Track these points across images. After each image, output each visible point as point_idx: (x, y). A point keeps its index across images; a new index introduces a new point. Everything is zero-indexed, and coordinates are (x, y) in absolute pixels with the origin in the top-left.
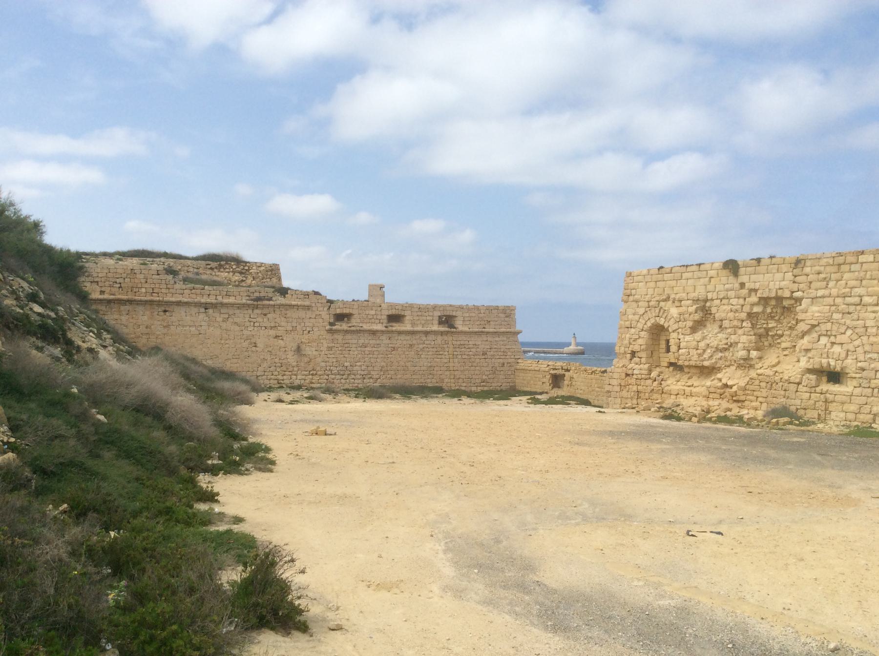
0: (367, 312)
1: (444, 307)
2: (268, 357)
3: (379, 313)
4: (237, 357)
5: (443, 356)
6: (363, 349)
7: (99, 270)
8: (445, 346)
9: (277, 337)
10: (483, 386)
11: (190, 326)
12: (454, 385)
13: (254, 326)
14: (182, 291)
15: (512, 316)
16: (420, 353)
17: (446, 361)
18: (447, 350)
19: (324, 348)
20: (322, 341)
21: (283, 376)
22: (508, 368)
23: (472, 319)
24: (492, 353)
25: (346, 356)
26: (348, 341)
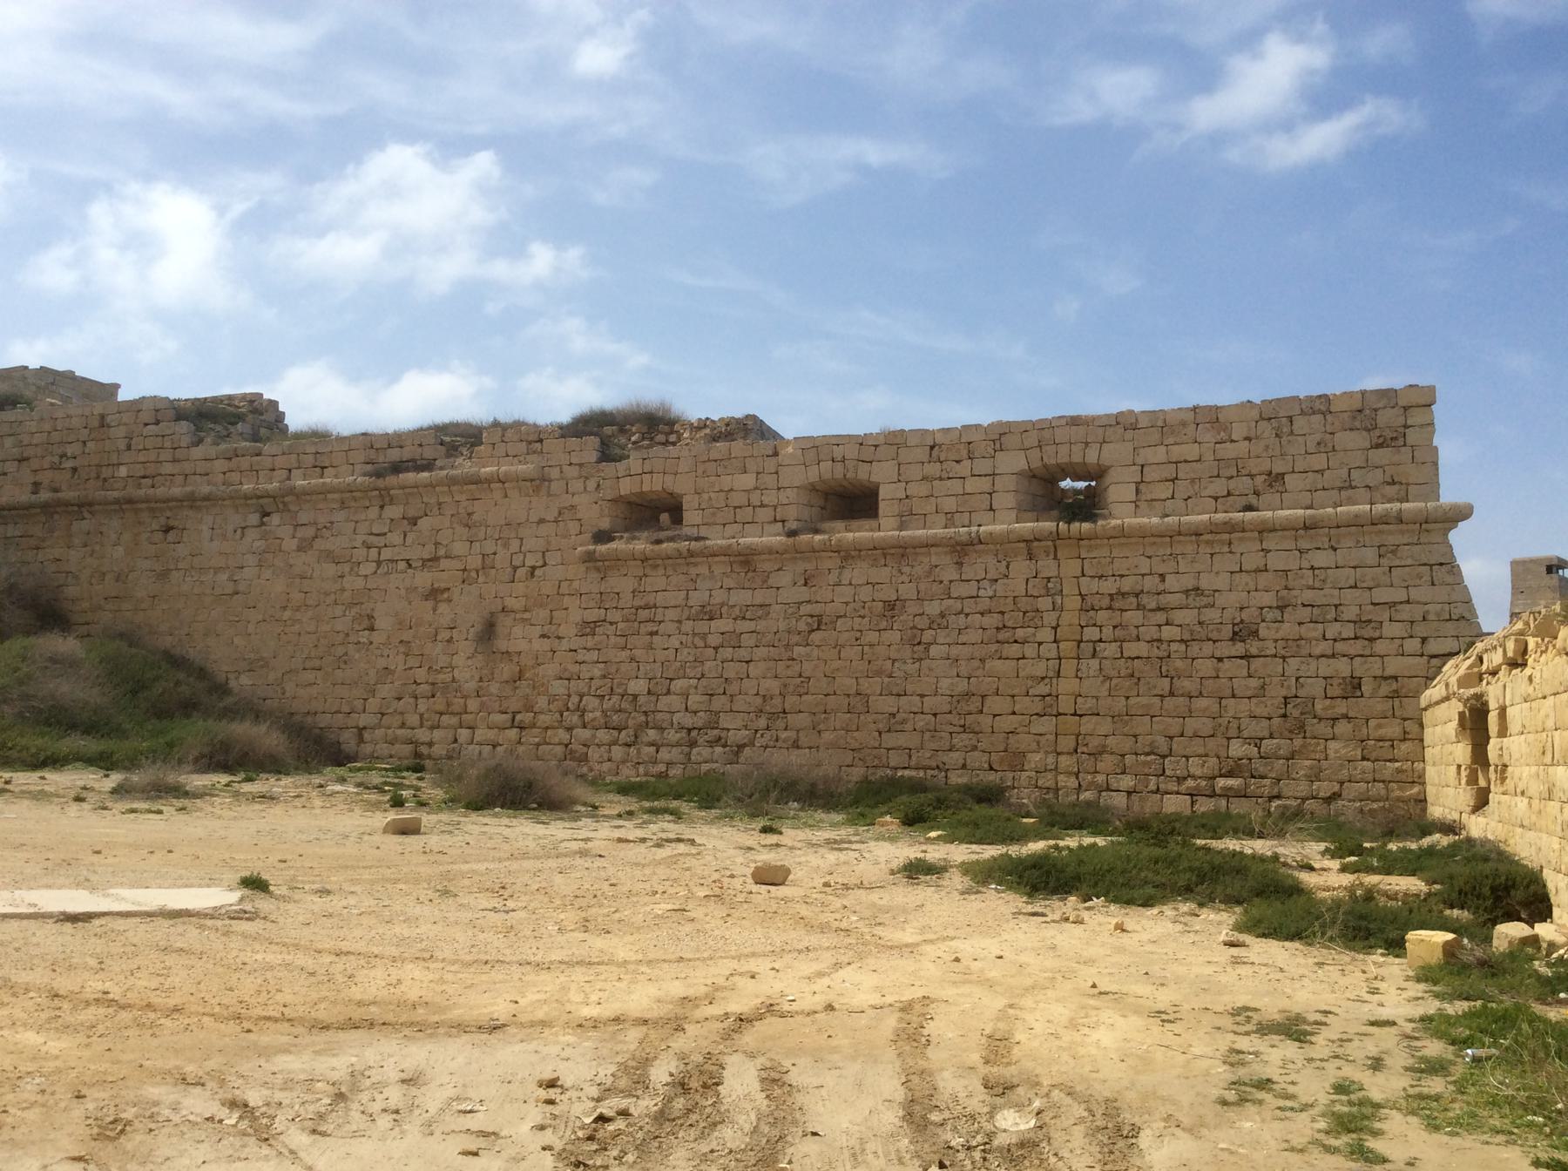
0: (726, 482)
1: (1043, 431)
2: (397, 662)
3: (770, 480)
4: (317, 663)
5: (1030, 650)
6: (702, 627)
7: (32, 425)
8: (1044, 603)
9: (434, 594)
10: (1228, 794)
11: (217, 570)
12: (1072, 782)
13: (379, 563)
14: (209, 464)
15: (1413, 435)
16: (928, 636)
17: (1040, 669)
18: (1051, 618)
19: (568, 630)
20: (567, 601)
21: (432, 728)
22: (1380, 706)
24: (1287, 629)
25: (638, 653)
26: (650, 599)
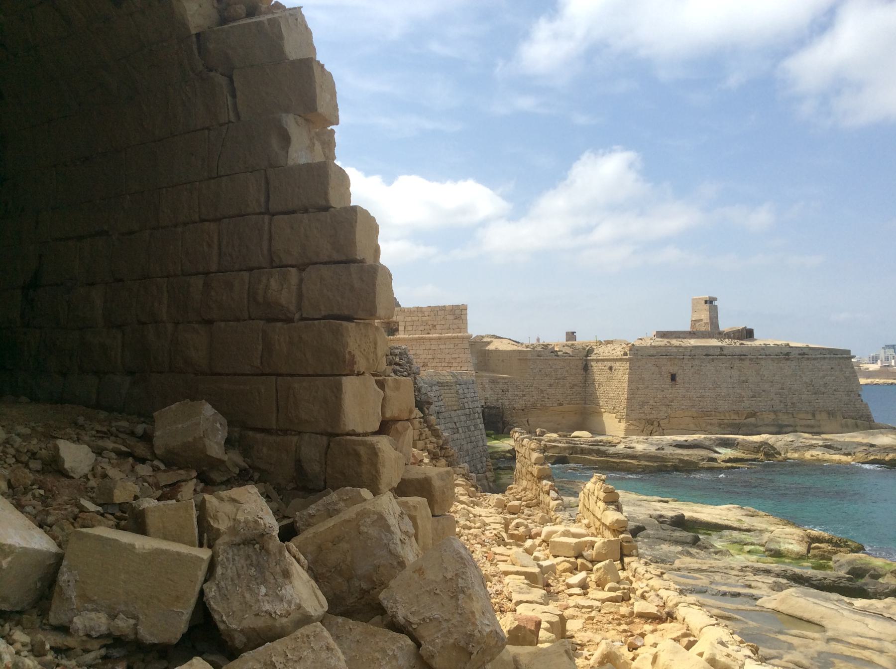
23: (415, 323)
24: (433, 364)
